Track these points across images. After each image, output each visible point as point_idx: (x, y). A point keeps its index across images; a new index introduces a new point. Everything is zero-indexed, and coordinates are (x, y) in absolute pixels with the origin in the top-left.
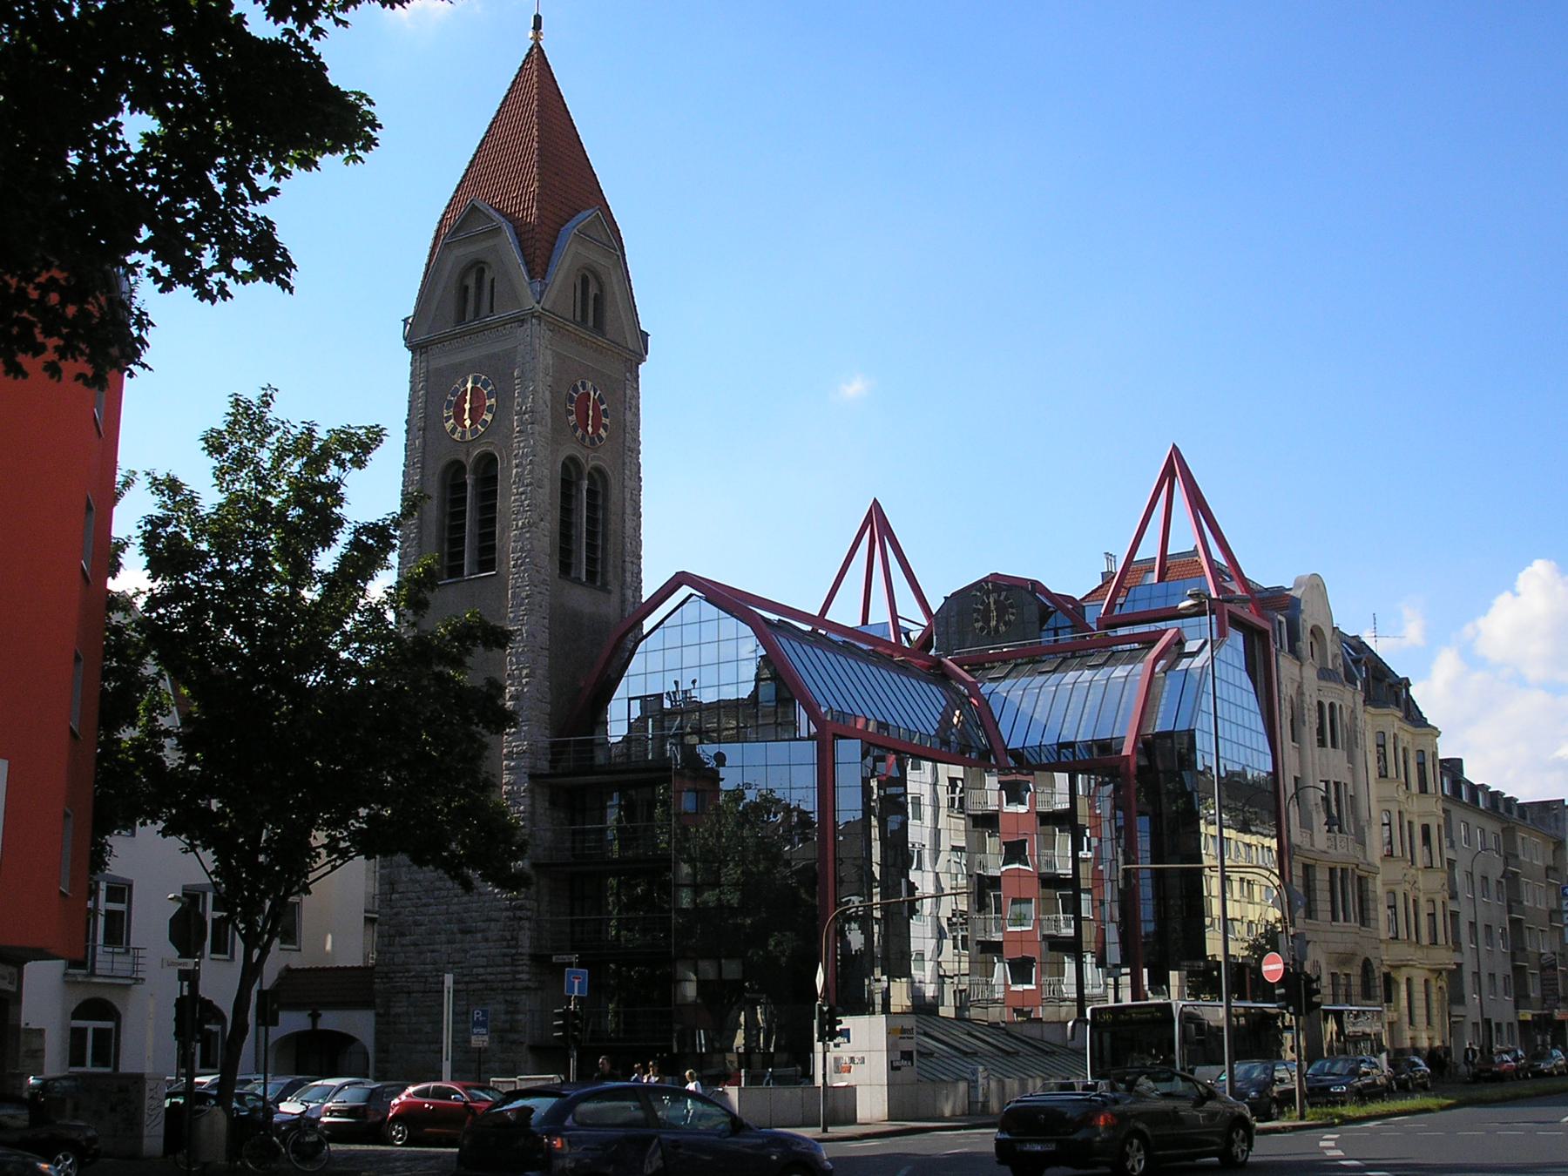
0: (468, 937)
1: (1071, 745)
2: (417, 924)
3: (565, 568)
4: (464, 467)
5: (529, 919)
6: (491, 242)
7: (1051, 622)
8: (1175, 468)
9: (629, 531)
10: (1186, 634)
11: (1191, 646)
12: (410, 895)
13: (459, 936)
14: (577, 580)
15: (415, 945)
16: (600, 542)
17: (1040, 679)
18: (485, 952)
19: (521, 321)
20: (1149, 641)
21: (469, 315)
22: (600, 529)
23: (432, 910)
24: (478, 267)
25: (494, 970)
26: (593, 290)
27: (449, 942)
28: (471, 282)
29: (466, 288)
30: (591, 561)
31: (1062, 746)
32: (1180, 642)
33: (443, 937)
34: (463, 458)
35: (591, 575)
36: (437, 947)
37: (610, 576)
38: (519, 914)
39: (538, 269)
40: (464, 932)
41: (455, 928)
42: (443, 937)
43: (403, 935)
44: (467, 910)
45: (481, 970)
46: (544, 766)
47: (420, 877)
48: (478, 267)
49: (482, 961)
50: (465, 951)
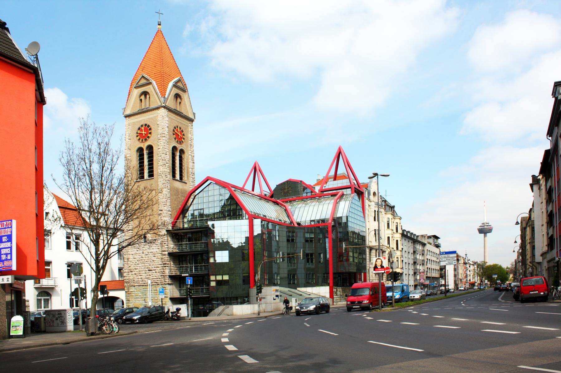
1: (314, 221)
3: (174, 176)
7: (306, 191)
8: (339, 153)
14: (177, 180)
19: (158, 108)
23: (140, 265)
29: (141, 100)
31: (311, 221)
33: (144, 272)
35: (181, 178)
41: (147, 269)
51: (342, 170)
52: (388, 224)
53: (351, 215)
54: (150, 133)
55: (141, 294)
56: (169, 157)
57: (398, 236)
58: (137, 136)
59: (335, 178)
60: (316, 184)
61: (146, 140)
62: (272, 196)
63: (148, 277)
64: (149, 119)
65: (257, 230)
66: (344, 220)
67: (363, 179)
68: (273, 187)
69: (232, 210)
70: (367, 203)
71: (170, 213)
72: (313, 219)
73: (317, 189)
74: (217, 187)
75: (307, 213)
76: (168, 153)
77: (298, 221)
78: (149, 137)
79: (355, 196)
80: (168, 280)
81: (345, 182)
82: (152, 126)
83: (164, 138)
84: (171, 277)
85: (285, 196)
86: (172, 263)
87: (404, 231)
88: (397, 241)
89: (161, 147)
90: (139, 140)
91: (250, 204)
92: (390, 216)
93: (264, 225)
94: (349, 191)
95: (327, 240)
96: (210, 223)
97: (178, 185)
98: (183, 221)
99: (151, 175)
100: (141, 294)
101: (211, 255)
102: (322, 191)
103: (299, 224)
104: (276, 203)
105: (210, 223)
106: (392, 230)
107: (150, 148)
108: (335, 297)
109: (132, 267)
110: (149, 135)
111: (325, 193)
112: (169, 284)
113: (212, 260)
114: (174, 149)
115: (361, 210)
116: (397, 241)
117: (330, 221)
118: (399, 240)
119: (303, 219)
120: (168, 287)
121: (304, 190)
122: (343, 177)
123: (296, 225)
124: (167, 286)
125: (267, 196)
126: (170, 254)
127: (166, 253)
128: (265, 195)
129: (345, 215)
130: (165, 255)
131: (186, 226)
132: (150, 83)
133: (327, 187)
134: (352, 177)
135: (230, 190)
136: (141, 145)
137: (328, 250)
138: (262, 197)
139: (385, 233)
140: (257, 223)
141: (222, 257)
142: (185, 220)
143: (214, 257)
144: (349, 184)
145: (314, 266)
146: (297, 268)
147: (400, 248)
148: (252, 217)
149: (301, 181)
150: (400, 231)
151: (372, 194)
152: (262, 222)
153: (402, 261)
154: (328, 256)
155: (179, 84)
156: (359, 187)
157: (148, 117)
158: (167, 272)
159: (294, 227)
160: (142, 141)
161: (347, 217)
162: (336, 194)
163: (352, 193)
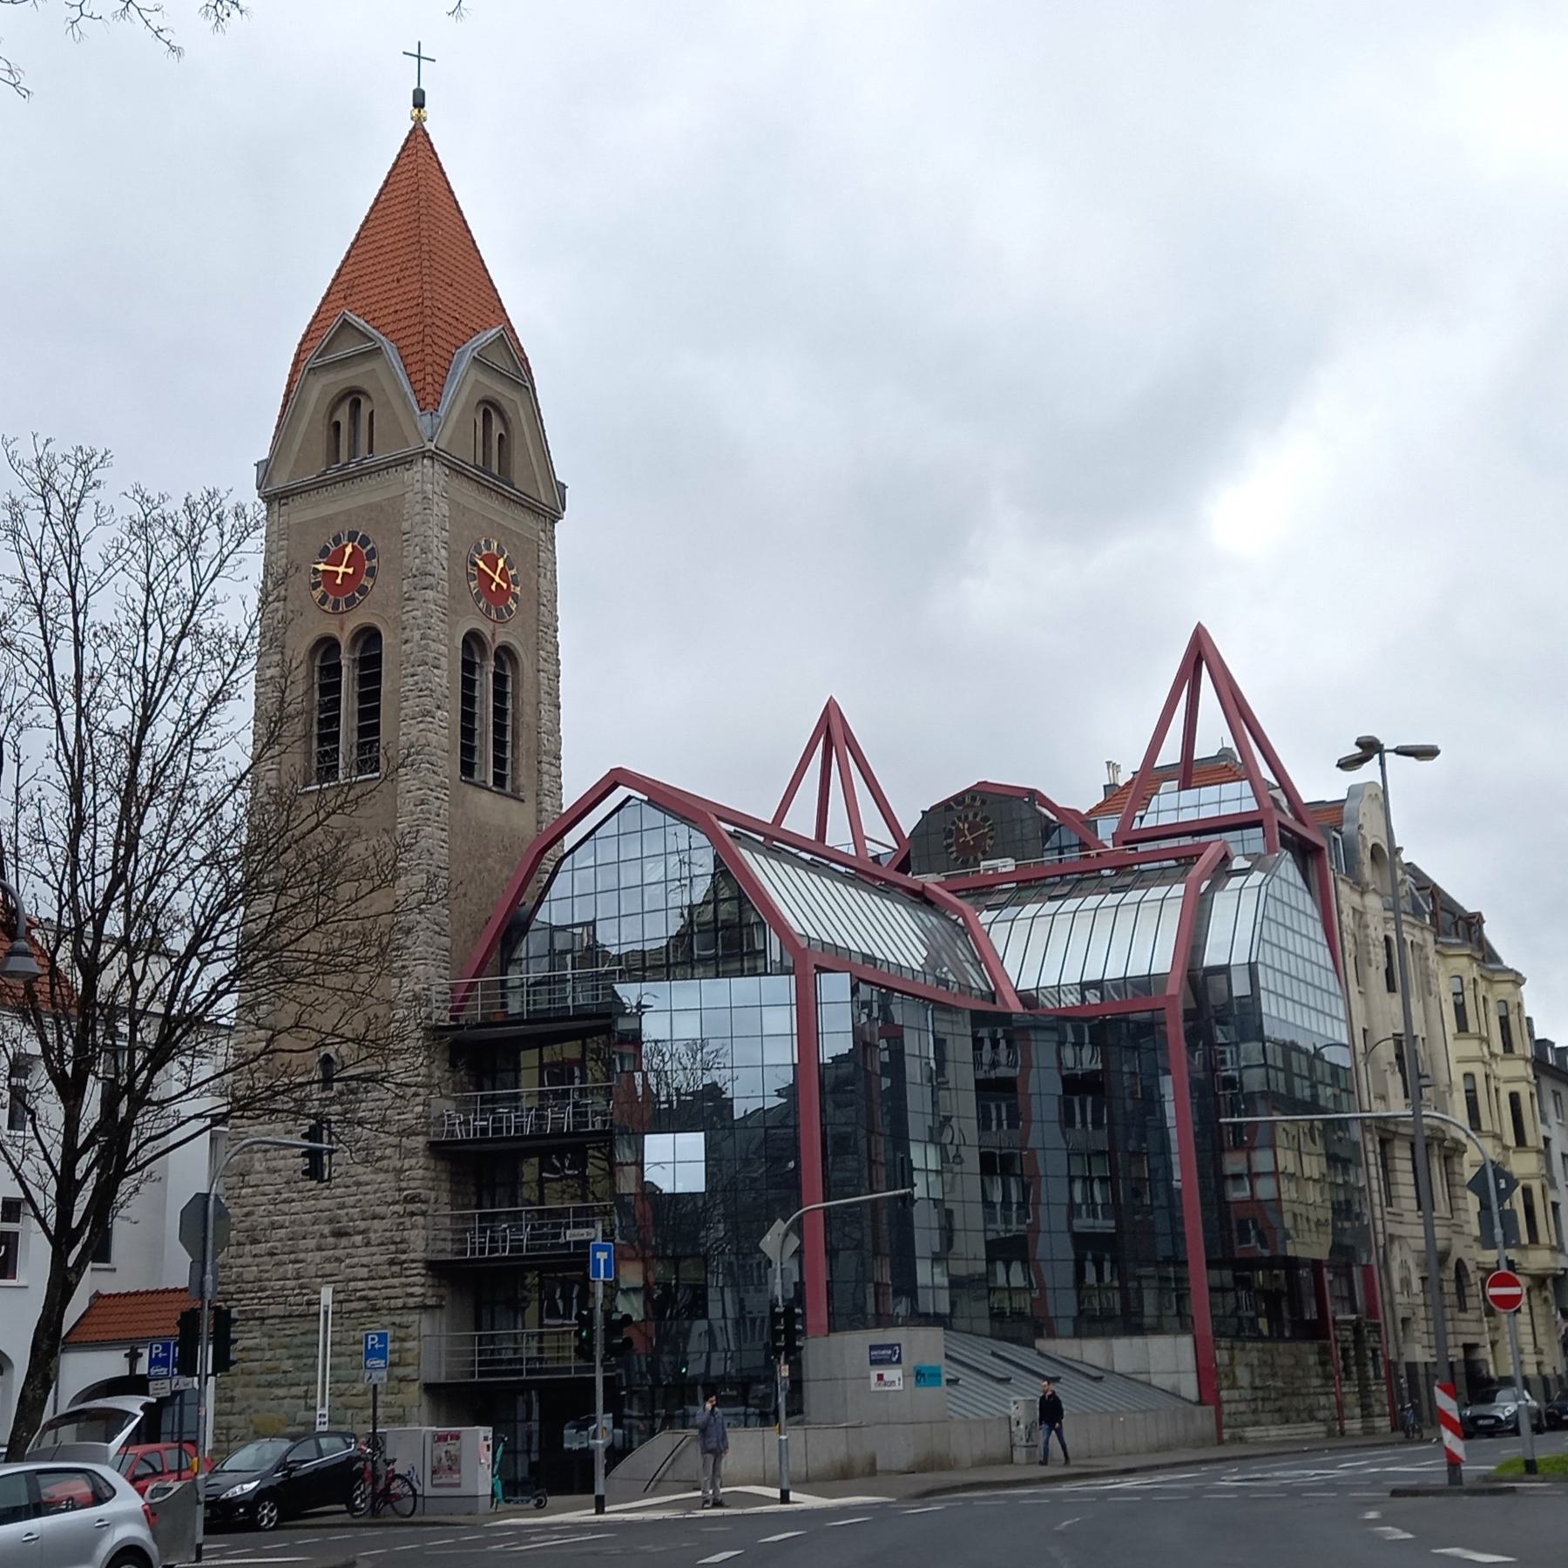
0: (344, 1241)
1: (1098, 985)
2: (274, 1226)
3: (467, 768)
4: (338, 645)
5: (424, 1214)
6: (368, 366)
8: (1200, 655)
9: (546, 724)
10: (1234, 849)
11: (1238, 863)
13: (331, 1240)
16: (509, 738)
17: (1051, 907)
18: (365, 1260)
19: (406, 462)
20: (1187, 859)
21: (344, 458)
22: (509, 722)
23: (296, 1206)
24: (353, 397)
25: (380, 1283)
26: (497, 428)
27: (320, 1249)
28: (343, 416)
29: (337, 425)
30: (499, 762)
31: (1085, 986)
32: (1226, 858)
33: (312, 1243)
34: (333, 631)
35: (499, 780)
36: (302, 1256)
37: (522, 780)
38: (411, 1208)
39: (430, 399)
40: (339, 1234)
41: (326, 1230)
42: (311, 1243)
43: (255, 1242)
44: (342, 1206)
45: (360, 1285)
46: (443, 1017)
47: (280, 1164)
48: (353, 397)
49: (364, 1272)
50: (339, 1260)
51: (1214, 735)
52: (1460, 1010)
53: (1267, 955)
54: (371, 572)
55: (287, 1365)
56: (446, 678)
57: (1515, 1072)
58: (315, 586)
59: (1190, 773)
60: (1099, 810)
61: (350, 602)
62: (904, 866)
64: (369, 507)
65: (836, 1041)
66: (1240, 987)
67: (1318, 782)
68: (908, 822)
69: (726, 934)
70: (1347, 897)
71: (446, 941)
72: (1093, 974)
73: (1106, 828)
74: (655, 817)
75: (1065, 949)
76: (444, 662)
77: (1028, 983)
78: (363, 590)
79: (1288, 868)
80: (418, 1286)
81: (1233, 798)
82: (377, 542)
83: (430, 594)
84: (431, 1266)
85: (965, 864)
86: (445, 1197)
87: (1542, 1044)
88: (1514, 1098)
89: (417, 634)
90: (323, 601)
91: (802, 902)
92: (1471, 971)
93: (866, 1004)
94: (1254, 839)
95: (1167, 1086)
96: (628, 992)
97: (485, 803)
98: (503, 984)
99: (368, 757)
100: (287, 1365)
101: (624, 1154)
102: (1129, 838)
103: (1028, 999)
104: (922, 899)
105: (628, 992)
106: (1485, 1041)
107: (369, 637)
108: (1224, 1394)
109: (260, 1219)
110: (366, 581)
111: (1142, 847)
112: (424, 1308)
113: (627, 1186)
114: (473, 640)
115: (1321, 937)
116: (1514, 1098)
117: (1173, 988)
118: (1524, 1090)
119: (1050, 979)
120: (423, 1325)
121: (1046, 836)
122: (1220, 770)
123: (1015, 1006)
124: (413, 1317)
125: (884, 862)
126: (437, 1149)
127: (419, 1142)
128: (876, 859)
129: (1240, 957)
130: (411, 1153)
131: (515, 1006)
132: (376, 352)
133: (1150, 822)
134: (1266, 773)
135: (714, 837)
136: (330, 627)
137: (1173, 1134)
138: (862, 874)
139: (1455, 1058)
140: (834, 987)
141: (675, 1162)
142: (513, 977)
143: (640, 1164)
144: (1250, 805)
146: (1035, 1229)
147: (1532, 1139)
148: (808, 962)
149: (1033, 793)
150: (1524, 1048)
151: (1366, 856)
152: (855, 990)
153: (1555, 1206)
154: (1177, 1175)
155: (500, 362)
156: (1299, 819)
157: (361, 500)
158: (418, 1242)
159: (1005, 1018)
160: (336, 605)
161: (1252, 968)
162: (1192, 858)
163: (1271, 849)
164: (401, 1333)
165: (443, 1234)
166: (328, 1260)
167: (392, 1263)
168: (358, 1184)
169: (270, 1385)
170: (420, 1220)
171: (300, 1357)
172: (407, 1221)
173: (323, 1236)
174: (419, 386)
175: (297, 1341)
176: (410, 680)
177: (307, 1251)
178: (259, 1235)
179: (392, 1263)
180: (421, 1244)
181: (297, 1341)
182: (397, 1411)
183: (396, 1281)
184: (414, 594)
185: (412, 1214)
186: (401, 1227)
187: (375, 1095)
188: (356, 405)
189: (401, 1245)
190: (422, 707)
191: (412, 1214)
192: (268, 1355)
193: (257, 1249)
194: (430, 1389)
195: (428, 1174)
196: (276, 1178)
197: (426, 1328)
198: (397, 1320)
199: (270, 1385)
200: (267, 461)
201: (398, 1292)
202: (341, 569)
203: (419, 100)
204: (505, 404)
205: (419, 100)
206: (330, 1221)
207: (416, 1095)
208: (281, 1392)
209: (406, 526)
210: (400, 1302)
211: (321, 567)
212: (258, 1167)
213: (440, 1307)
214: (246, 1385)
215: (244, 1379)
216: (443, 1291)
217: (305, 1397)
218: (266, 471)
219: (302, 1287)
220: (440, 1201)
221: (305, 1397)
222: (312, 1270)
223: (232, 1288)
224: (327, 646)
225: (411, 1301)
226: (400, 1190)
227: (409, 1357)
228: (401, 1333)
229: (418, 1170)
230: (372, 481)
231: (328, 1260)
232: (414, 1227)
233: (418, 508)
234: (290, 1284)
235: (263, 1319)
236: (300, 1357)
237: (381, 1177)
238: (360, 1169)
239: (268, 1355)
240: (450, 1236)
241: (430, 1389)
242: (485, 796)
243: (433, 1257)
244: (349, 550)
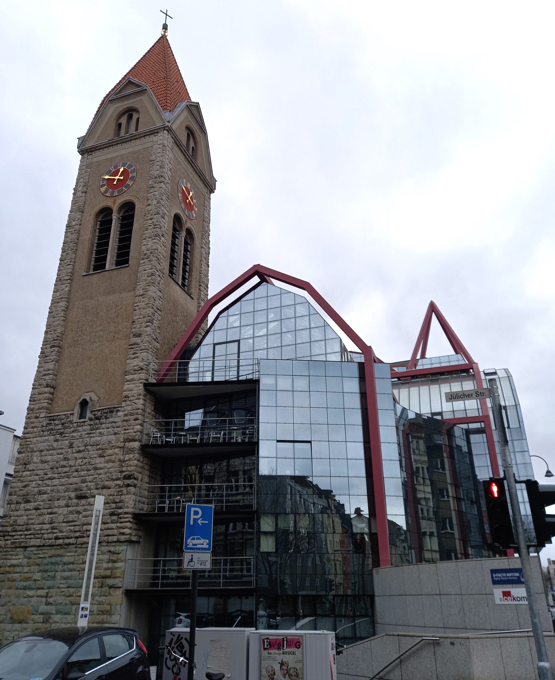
0: (83, 502)
2: (40, 493)
5: (135, 486)
12: (39, 472)
13: (75, 501)
15: (37, 509)
23: (56, 482)
27: (67, 506)
28: (124, 120)
33: (62, 503)
36: (55, 510)
40: (79, 497)
41: (73, 495)
42: (62, 503)
43: (28, 502)
44: (84, 481)
47: (49, 458)
50: (78, 512)
55: (37, 576)
63: (71, 517)
71: (158, 346)
78: (128, 187)
80: (128, 529)
86: (146, 479)
89: (155, 202)
99: (123, 259)
100: (37, 576)
107: (128, 208)
110: (129, 182)
112: (130, 542)
120: (128, 553)
124: (123, 547)
126: (145, 450)
130: (131, 451)
136: (108, 203)
145: (498, 602)
157: (130, 150)
158: (131, 502)
164: (114, 557)
165: (144, 499)
166: (71, 512)
167: (112, 514)
168: (96, 469)
169: (25, 588)
170: (132, 489)
171: (47, 571)
172: (124, 490)
173: (70, 498)
174: (163, 105)
175: (45, 561)
176: (150, 222)
177: (59, 507)
178: (29, 498)
179: (112, 514)
180: (131, 503)
181: (45, 561)
182: (108, 607)
183: (114, 526)
184: (155, 185)
185: (128, 485)
186: (120, 493)
187: (111, 420)
188: (130, 117)
189: (119, 504)
190: (151, 242)
191: (128, 485)
192: (26, 569)
193: (28, 506)
194: (129, 593)
195: (139, 464)
196: (46, 466)
197: (129, 555)
198: (112, 549)
199: (25, 588)
200: (84, 137)
201: (115, 532)
202: (117, 178)
203: (165, 27)
204: (196, 135)
205: (165, 27)
206: (76, 490)
207: (136, 419)
208: (31, 593)
209: (153, 158)
210: (115, 538)
211: (107, 177)
212: (35, 459)
213: (138, 542)
214: (10, 588)
215: (8, 584)
216: (140, 533)
217: (46, 597)
218: (82, 141)
219: (53, 528)
220: (143, 480)
221: (46, 597)
222: (61, 518)
223: (9, 529)
224: (106, 212)
225: (122, 538)
226: (122, 472)
227: (118, 573)
228: (114, 557)
229: (134, 462)
230: (138, 142)
231: (71, 512)
232: (128, 493)
233: (160, 150)
234: (46, 526)
235: (25, 547)
236: (47, 571)
237: (110, 465)
238: (98, 460)
239: (26, 569)
240: (146, 501)
241: (129, 593)
242: (178, 288)
243: (137, 511)
244: (122, 170)
